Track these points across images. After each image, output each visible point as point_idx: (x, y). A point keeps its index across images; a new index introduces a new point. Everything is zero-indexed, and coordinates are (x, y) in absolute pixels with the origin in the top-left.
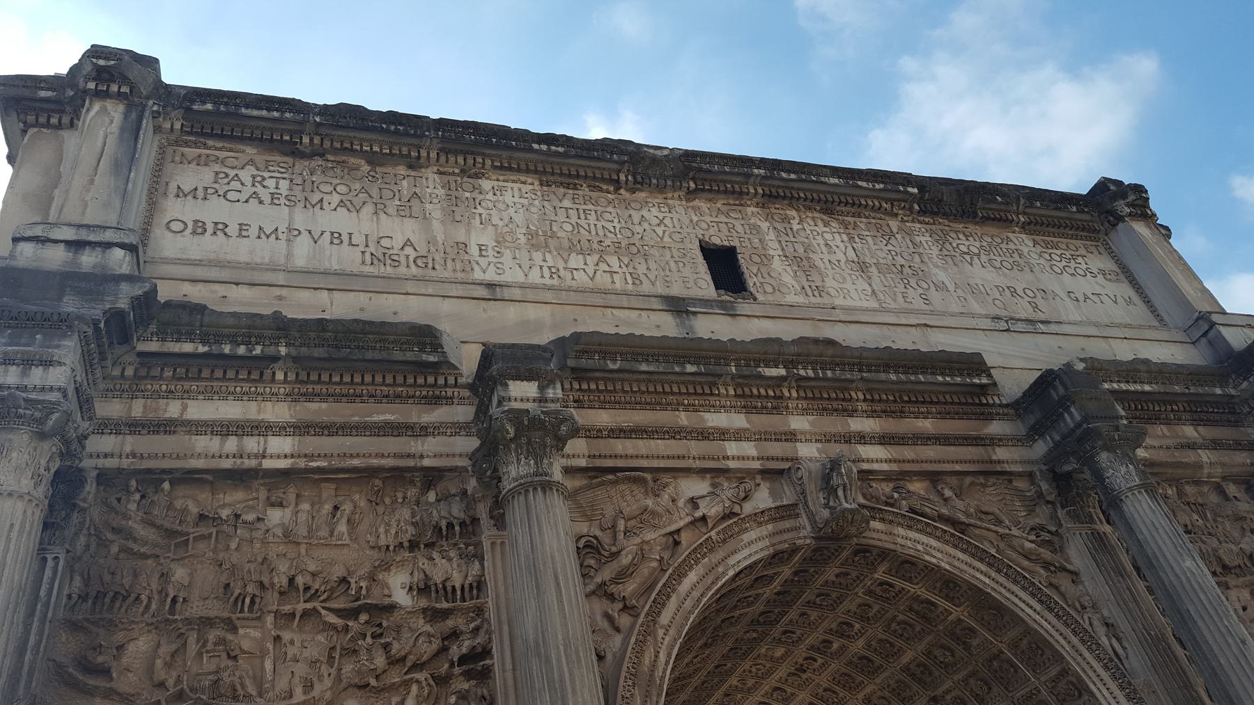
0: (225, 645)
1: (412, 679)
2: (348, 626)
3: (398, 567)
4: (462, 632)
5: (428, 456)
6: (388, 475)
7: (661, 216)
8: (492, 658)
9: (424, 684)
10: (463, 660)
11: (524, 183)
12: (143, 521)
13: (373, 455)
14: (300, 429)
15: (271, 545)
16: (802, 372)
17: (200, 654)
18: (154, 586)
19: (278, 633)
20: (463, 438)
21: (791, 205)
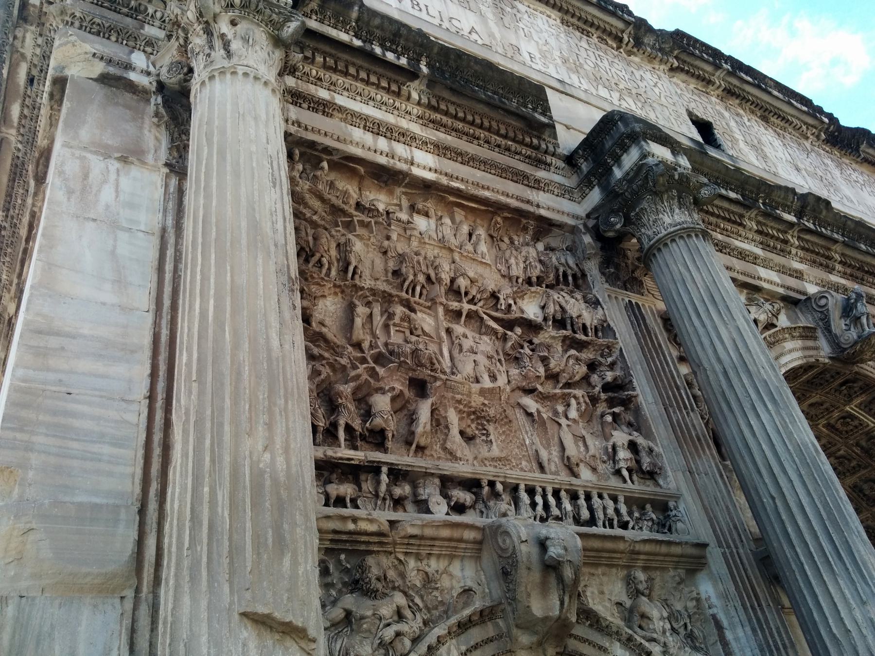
0: (409, 322)
1: (569, 394)
2: (506, 334)
3: (530, 298)
4: (601, 364)
5: (543, 208)
6: (510, 216)
7: (655, 80)
8: (634, 389)
9: (581, 400)
10: (606, 387)
11: (549, 17)
12: (310, 191)
13: (500, 192)
14: (441, 150)
15: (427, 246)
16: (806, 223)
17: (386, 327)
18: (334, 253)
19: (450, 325)
20: (566, 201)
21: (740, 105)
